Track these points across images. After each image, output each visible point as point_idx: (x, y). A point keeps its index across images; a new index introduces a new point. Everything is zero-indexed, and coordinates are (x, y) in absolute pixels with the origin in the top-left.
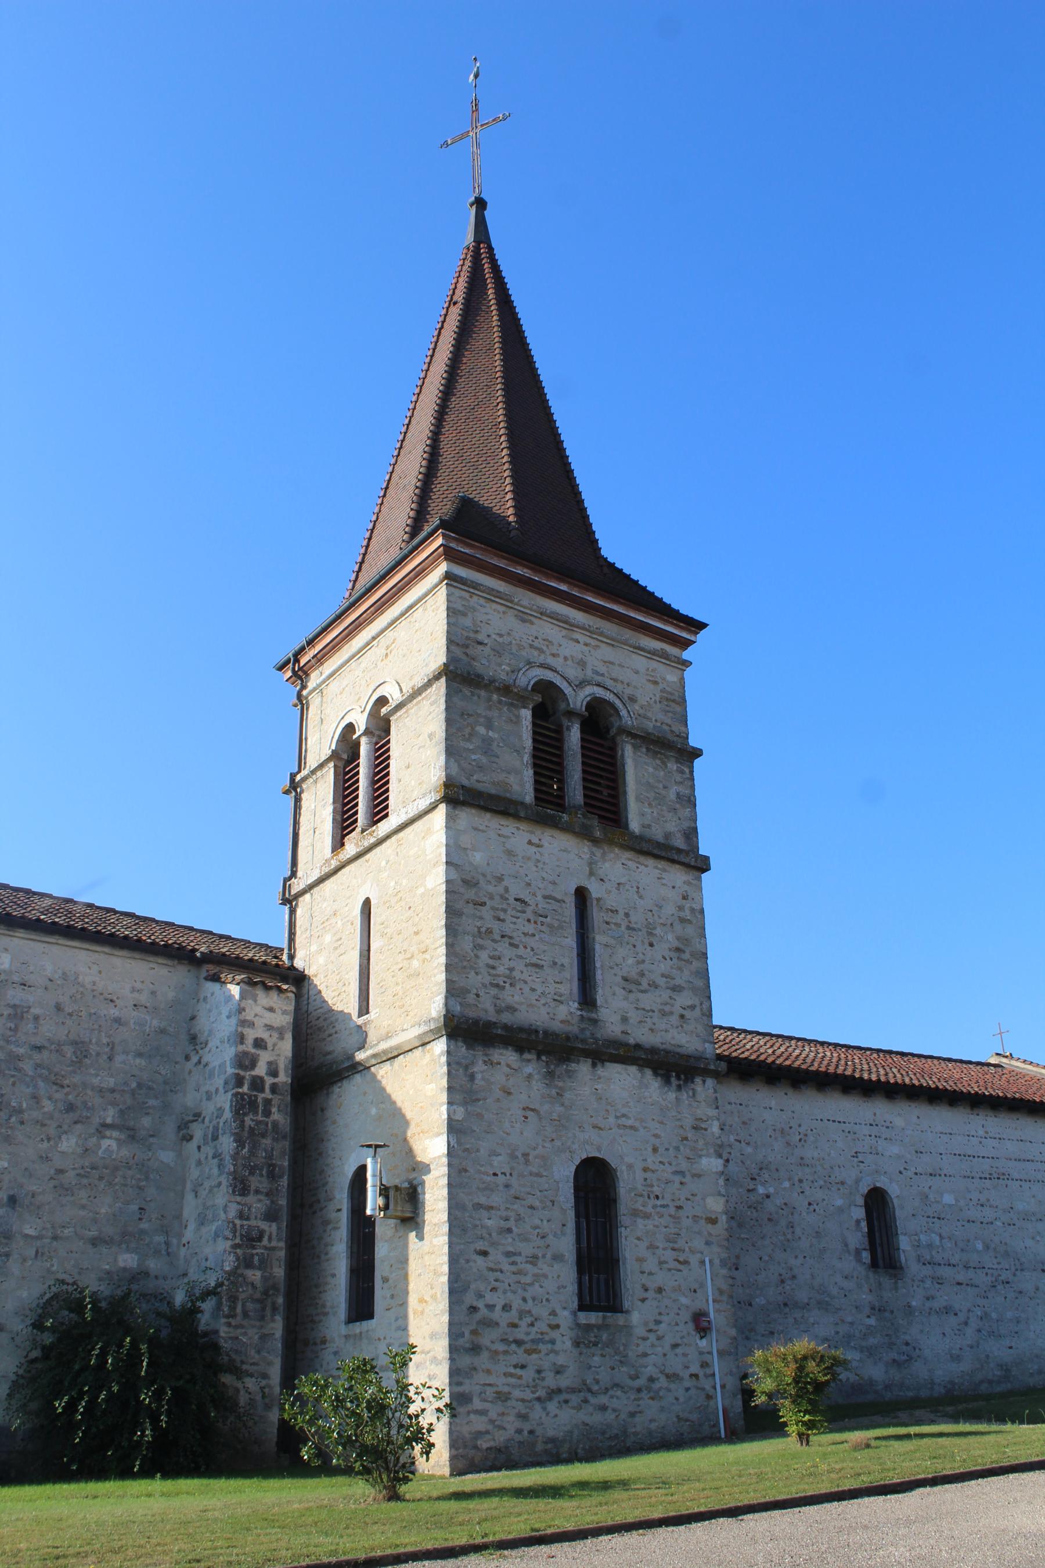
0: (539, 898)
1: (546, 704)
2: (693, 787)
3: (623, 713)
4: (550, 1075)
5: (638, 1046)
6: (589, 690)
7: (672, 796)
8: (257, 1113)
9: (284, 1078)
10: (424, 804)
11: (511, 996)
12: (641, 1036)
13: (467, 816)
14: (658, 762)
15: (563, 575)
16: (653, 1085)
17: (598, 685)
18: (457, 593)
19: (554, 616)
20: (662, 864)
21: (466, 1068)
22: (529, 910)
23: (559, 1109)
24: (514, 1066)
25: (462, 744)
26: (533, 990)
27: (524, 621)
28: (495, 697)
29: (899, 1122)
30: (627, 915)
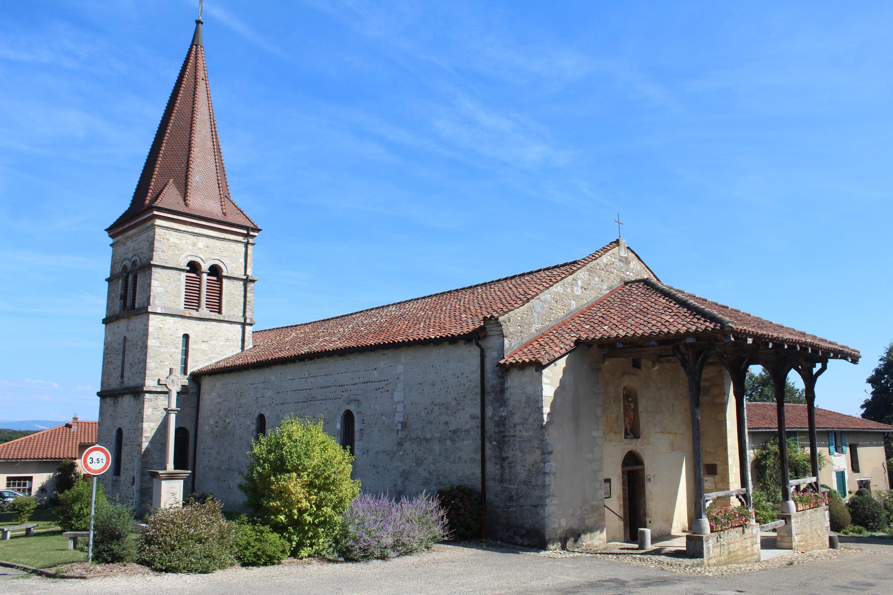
4: (114, 403)
16: (132, 399)
29: (273, 378)
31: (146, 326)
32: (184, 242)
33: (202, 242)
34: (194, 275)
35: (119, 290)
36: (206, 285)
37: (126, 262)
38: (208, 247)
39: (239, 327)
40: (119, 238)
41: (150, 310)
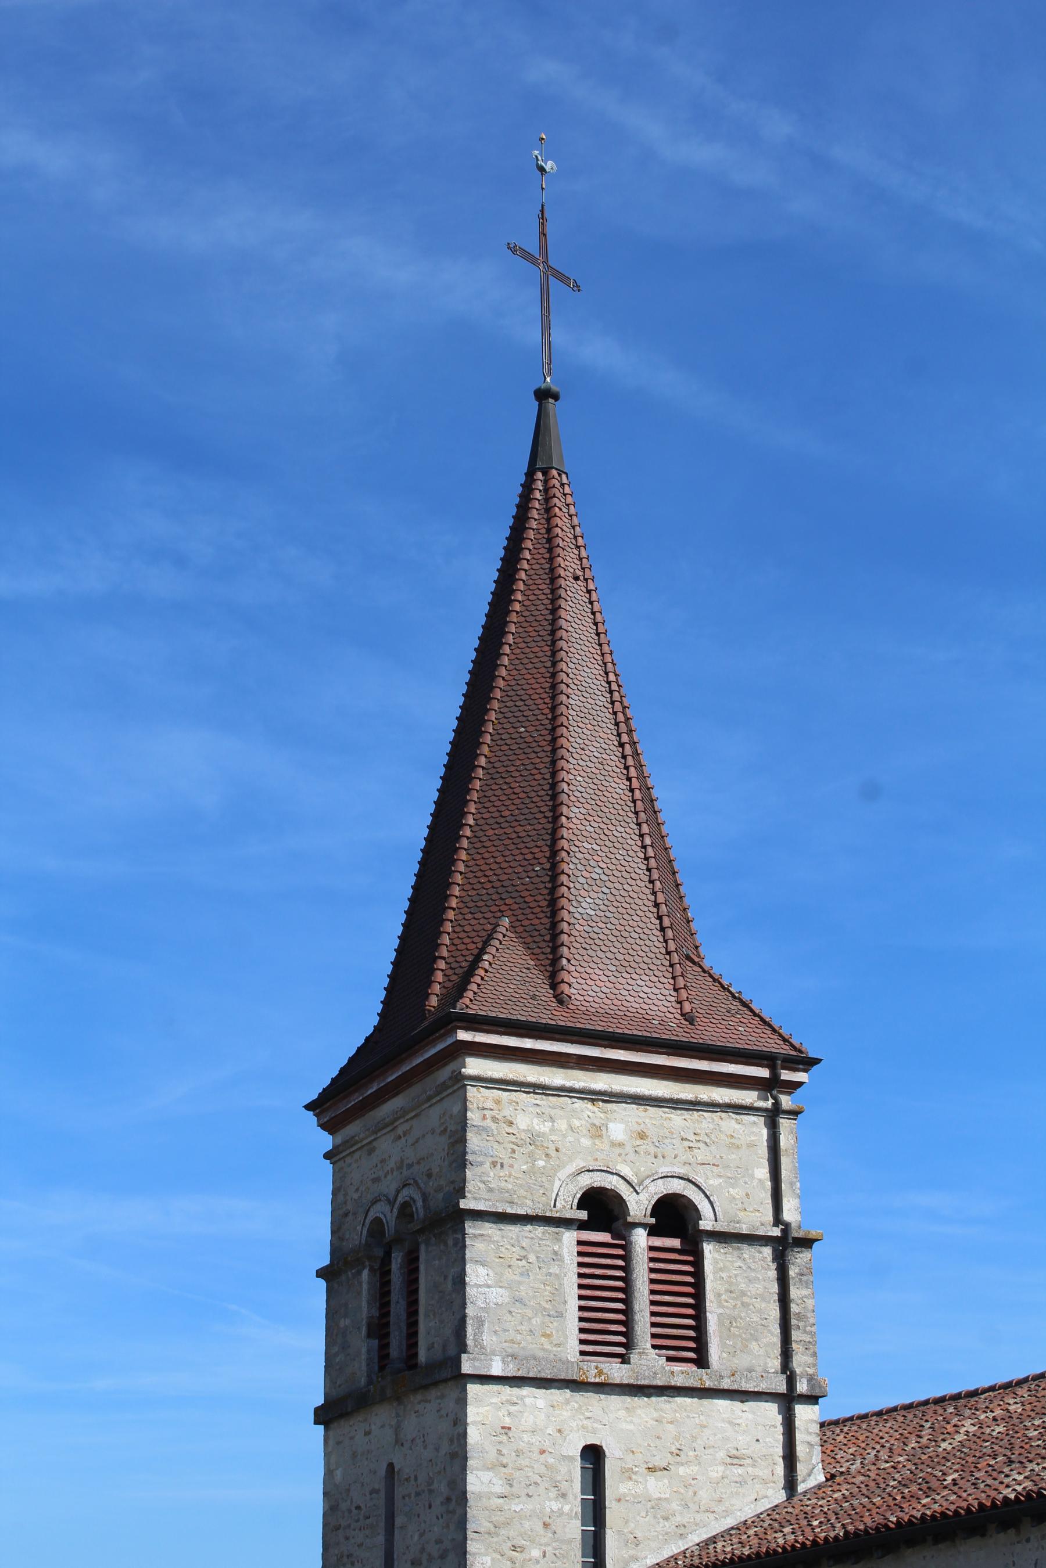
14: (442, 1247)
31: (460, 1422)
32: (562, 1125)
33: (621, 1122)
34: (604, 1237)
35: (363, 1306)
36: (644, 1265)
37: (380, 1210)
38: (642, 1136)
39: (771, 1411)
40: (352, 1129)
41: (466, 1368)
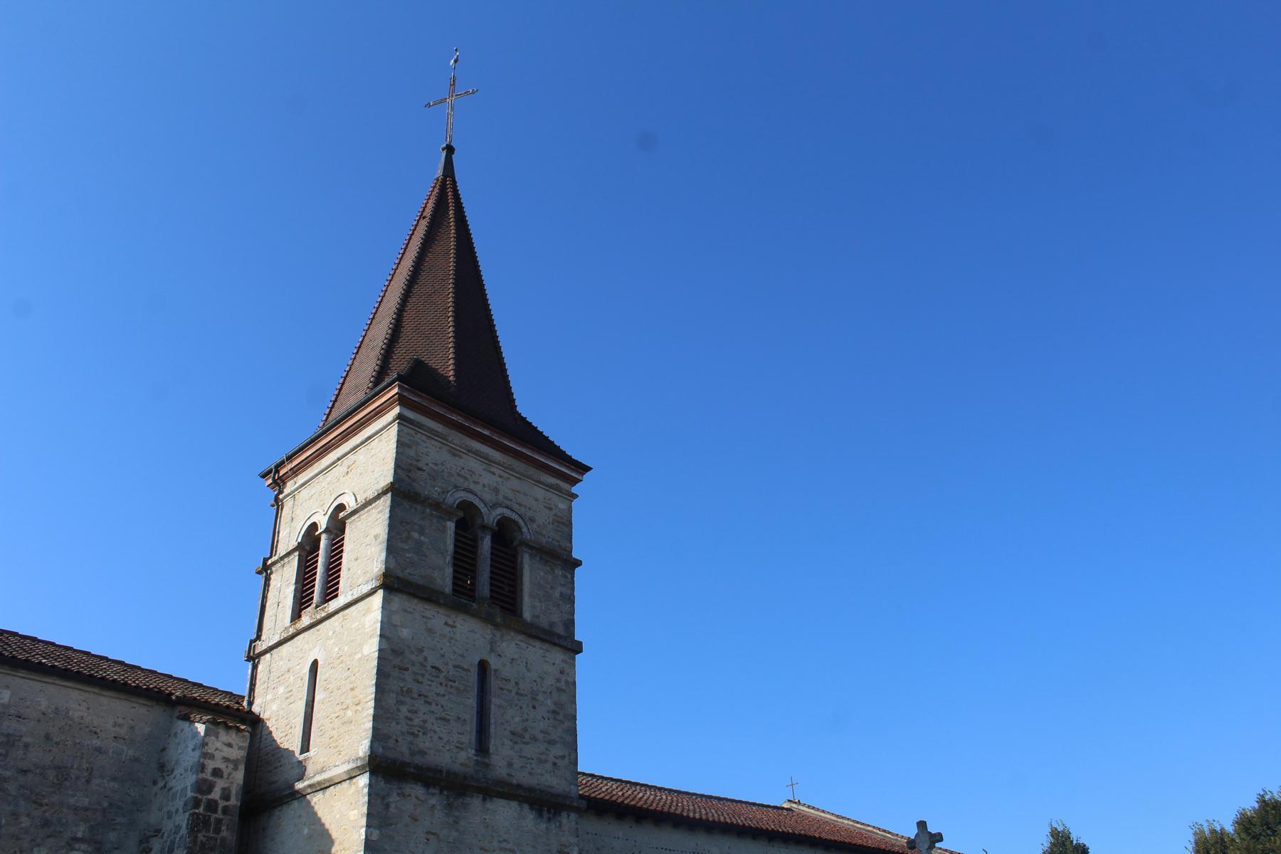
0: (450, 667)
1: (467, 518)
2: (573, 589)
3: (524, 529)
4: (450, 806)
5: (519, 786)
6: (499, 511)
7: (557, 595)
8: (208, 831)
9: (234, 801)
10: (366, 589)
11: (424, 743)
12: (522, 777)
13: (398, 601)
15: (488, 423)
16: (530, 816)
17: (507, 507)
18: (406, 430)
19: (477, 453)
20: (546, 646)
21: (383, 798)
22: (442, 676)
23: (455, 834)
24: (422, 798)
25: (400, 545)
26: (440, 738)
27: (455, 455)
28: (428, 510)
30: (517, 683)
